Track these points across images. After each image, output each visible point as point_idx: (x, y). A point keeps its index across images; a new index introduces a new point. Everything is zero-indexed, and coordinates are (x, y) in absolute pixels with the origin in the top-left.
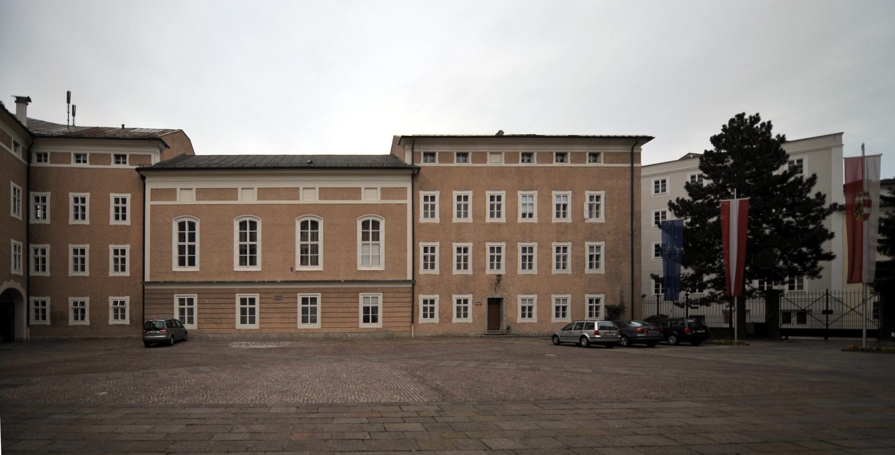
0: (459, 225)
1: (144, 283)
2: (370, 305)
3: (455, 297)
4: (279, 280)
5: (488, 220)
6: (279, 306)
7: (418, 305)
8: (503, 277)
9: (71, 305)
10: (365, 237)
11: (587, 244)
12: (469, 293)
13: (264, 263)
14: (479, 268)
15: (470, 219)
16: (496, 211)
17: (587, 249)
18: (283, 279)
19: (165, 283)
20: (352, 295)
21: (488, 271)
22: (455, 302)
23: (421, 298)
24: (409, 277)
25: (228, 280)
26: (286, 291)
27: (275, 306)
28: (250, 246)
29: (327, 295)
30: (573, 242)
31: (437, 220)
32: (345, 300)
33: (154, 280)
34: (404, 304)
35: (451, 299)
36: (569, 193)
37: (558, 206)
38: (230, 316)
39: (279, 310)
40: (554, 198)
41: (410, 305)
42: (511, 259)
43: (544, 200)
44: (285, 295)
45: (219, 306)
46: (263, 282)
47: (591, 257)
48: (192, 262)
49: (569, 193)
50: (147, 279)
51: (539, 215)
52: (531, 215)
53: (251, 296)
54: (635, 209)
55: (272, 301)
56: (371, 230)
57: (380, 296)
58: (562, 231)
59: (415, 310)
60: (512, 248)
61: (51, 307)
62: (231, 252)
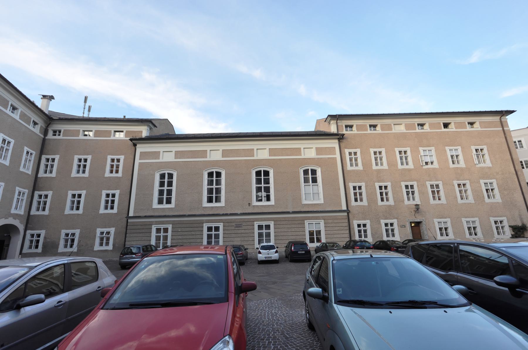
0: (379, 171)
1: (128, 217)
2: (315, 229)
3: (383, 222)
4: (239, 212)
5: (400, 166)
6: (239, 232)
7: (354, 228)
8: (420, 206)
9: (63, 236)
10: (306, 181)
11: (482, 182)
12: (394, 218)
13: (226, 201)
14: (398, 200)
15: (385, 166)
16: (404, 159)
17: (483, 185)
18: (242, 212)
19: (146, 217)
20: (299, 222)
21: (406, 202)
22: (383, 225)
23: (355, 223)
24: (344, 208)
25: (197, 213)
26: (244, 221)
27: (236, 231)
28: (216, 188)
29: (279, 223)
30: (470, 180)
31: (360, 167)
32: (293, 226)
33: (137, 215)
34: (342, 228)
35: (380, 223)
36: (459, 148)
37: (452, 156)
38: (199, 241)
39: (239, 235)
40: (448, 151)
41: (348, 228)
42: (423, 193)
43: (441, 154)
44: (244, 224)
45: (190, 233)
46: (226, 215)
47: (487, 190)
48: (169, 201)
49: (459, 148)
50: (131, 214)
51: (439, 163)
52: (432, 163)
53: (217, 225)
54: (514, 157)
55: (233, 228)
56: (311, 176)
57: (322, 222)
58: (459, 173)
59: (352, 233)
60: (422, 186)
61: (45, 238)
62: (201, 193)
